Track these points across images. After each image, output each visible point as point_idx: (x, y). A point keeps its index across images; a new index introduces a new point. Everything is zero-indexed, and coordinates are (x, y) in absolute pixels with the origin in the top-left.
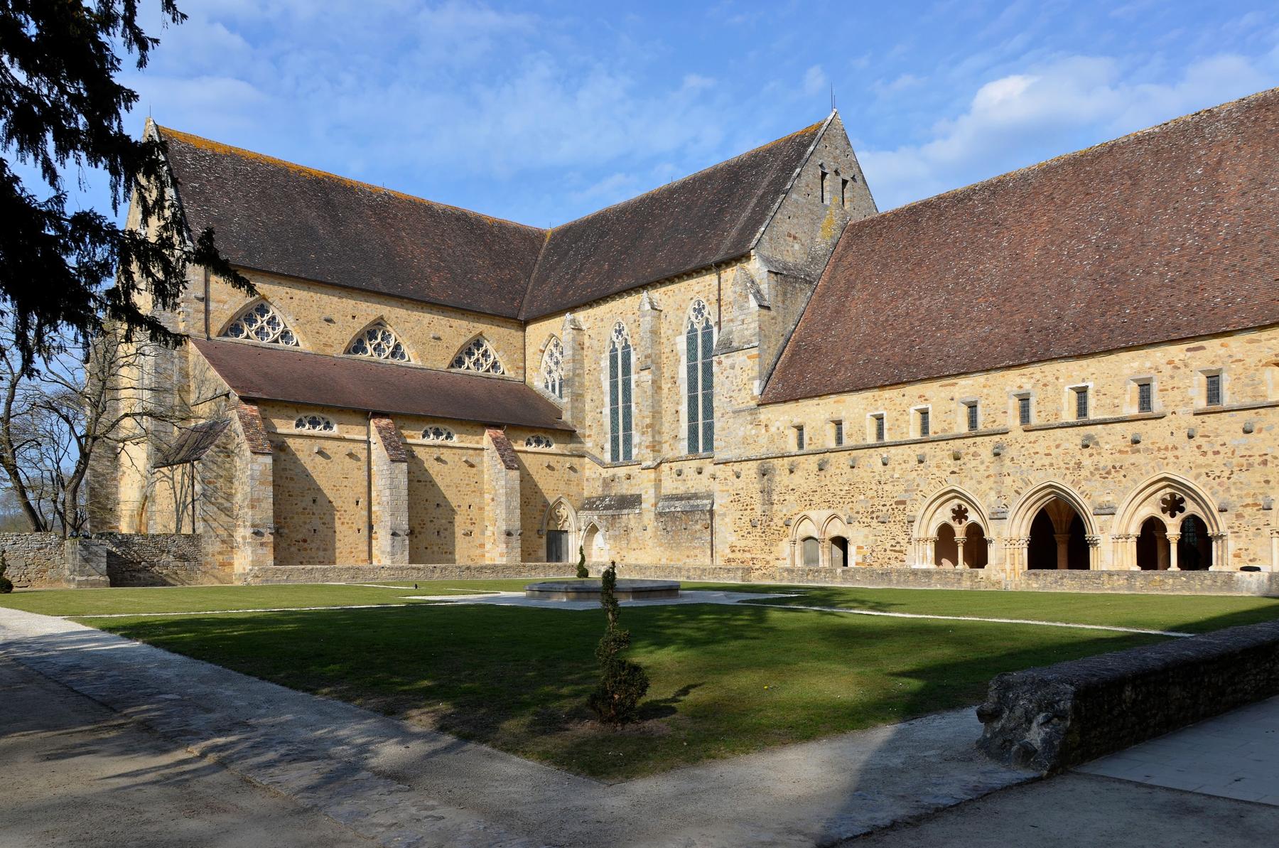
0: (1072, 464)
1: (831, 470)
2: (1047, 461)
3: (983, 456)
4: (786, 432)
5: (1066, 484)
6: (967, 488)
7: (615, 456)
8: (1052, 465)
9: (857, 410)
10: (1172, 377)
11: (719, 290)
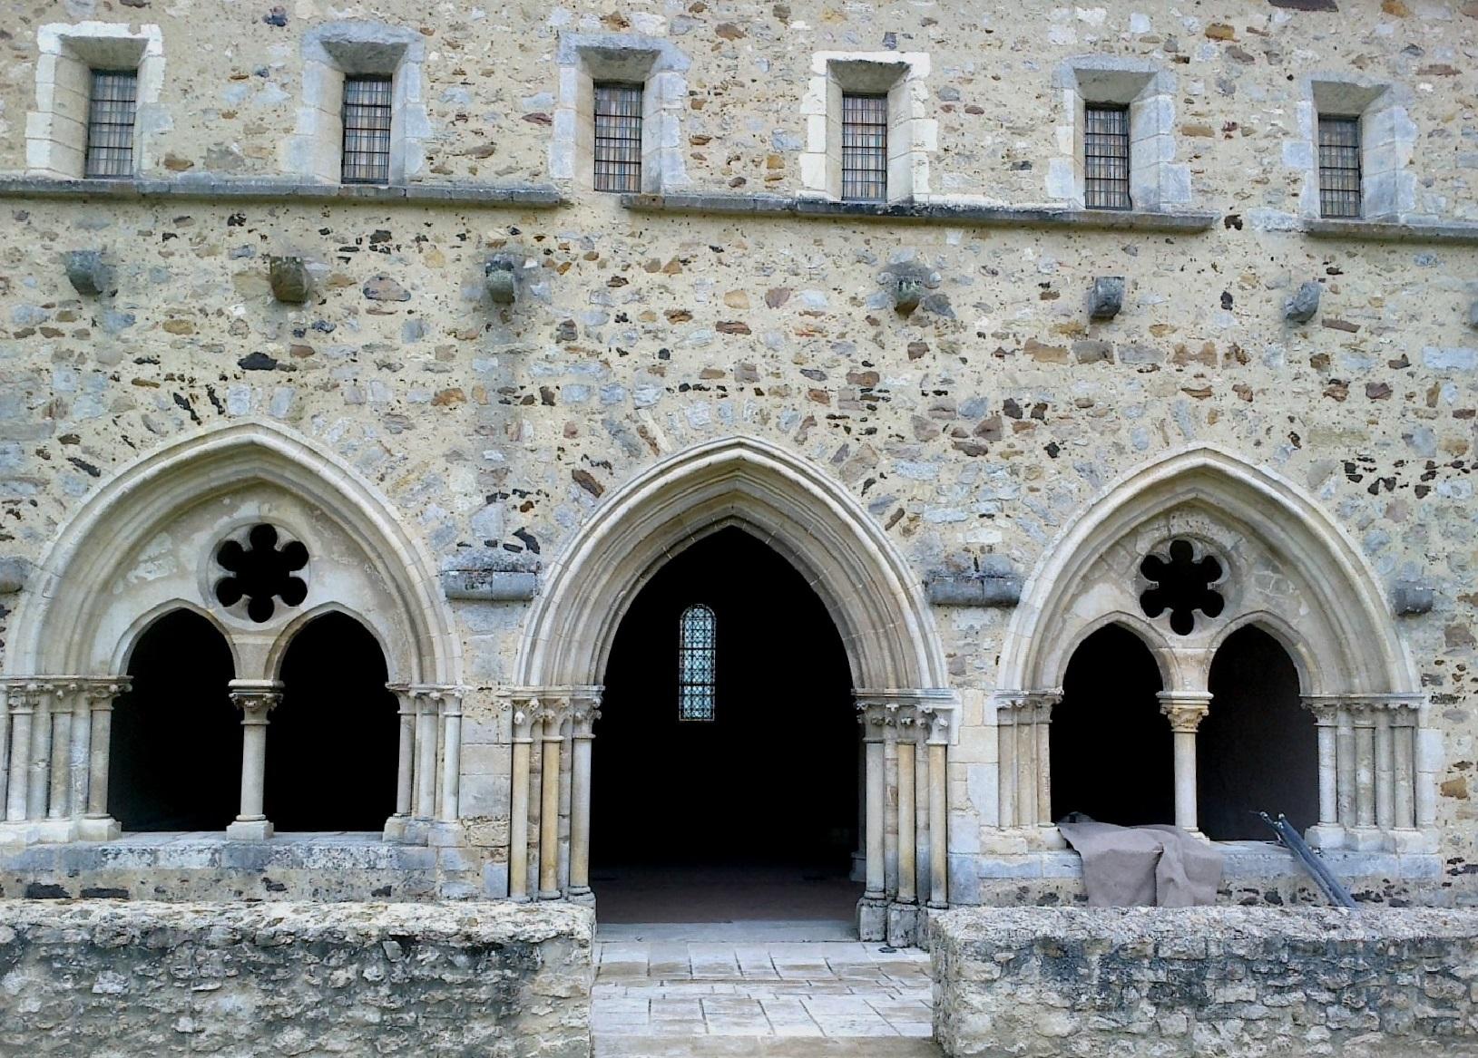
0: (836, 381)
2: (726, 354)
3: (423, 302)
5: (807, 456)
6: (328, 444)
8: (748, 373)
10: (1226, 89)
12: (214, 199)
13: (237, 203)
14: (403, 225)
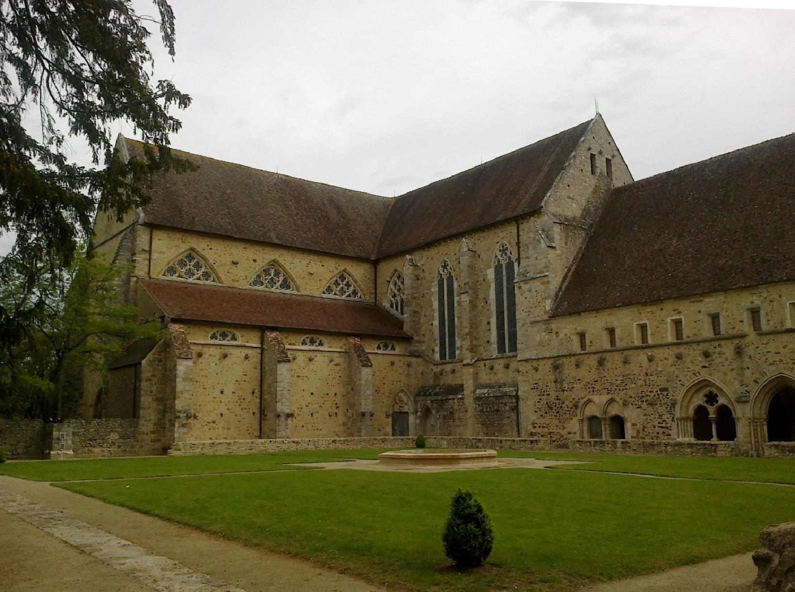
1: (608, 365)
2: (777, 358)
3: (727, 355)
4: (572, 337)
6: (716, 379)
7: (443, 355)
8: (781, 361)
9: (626, 322)
11: (518, 236)
12: (694, 342)
13: (698, 343)
14: (723, 343)
